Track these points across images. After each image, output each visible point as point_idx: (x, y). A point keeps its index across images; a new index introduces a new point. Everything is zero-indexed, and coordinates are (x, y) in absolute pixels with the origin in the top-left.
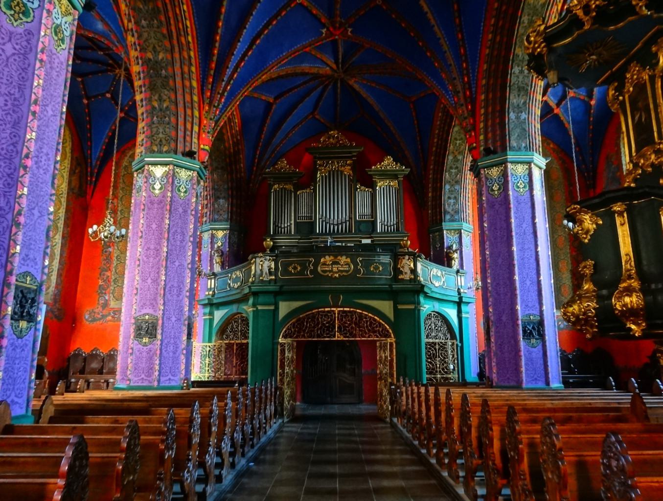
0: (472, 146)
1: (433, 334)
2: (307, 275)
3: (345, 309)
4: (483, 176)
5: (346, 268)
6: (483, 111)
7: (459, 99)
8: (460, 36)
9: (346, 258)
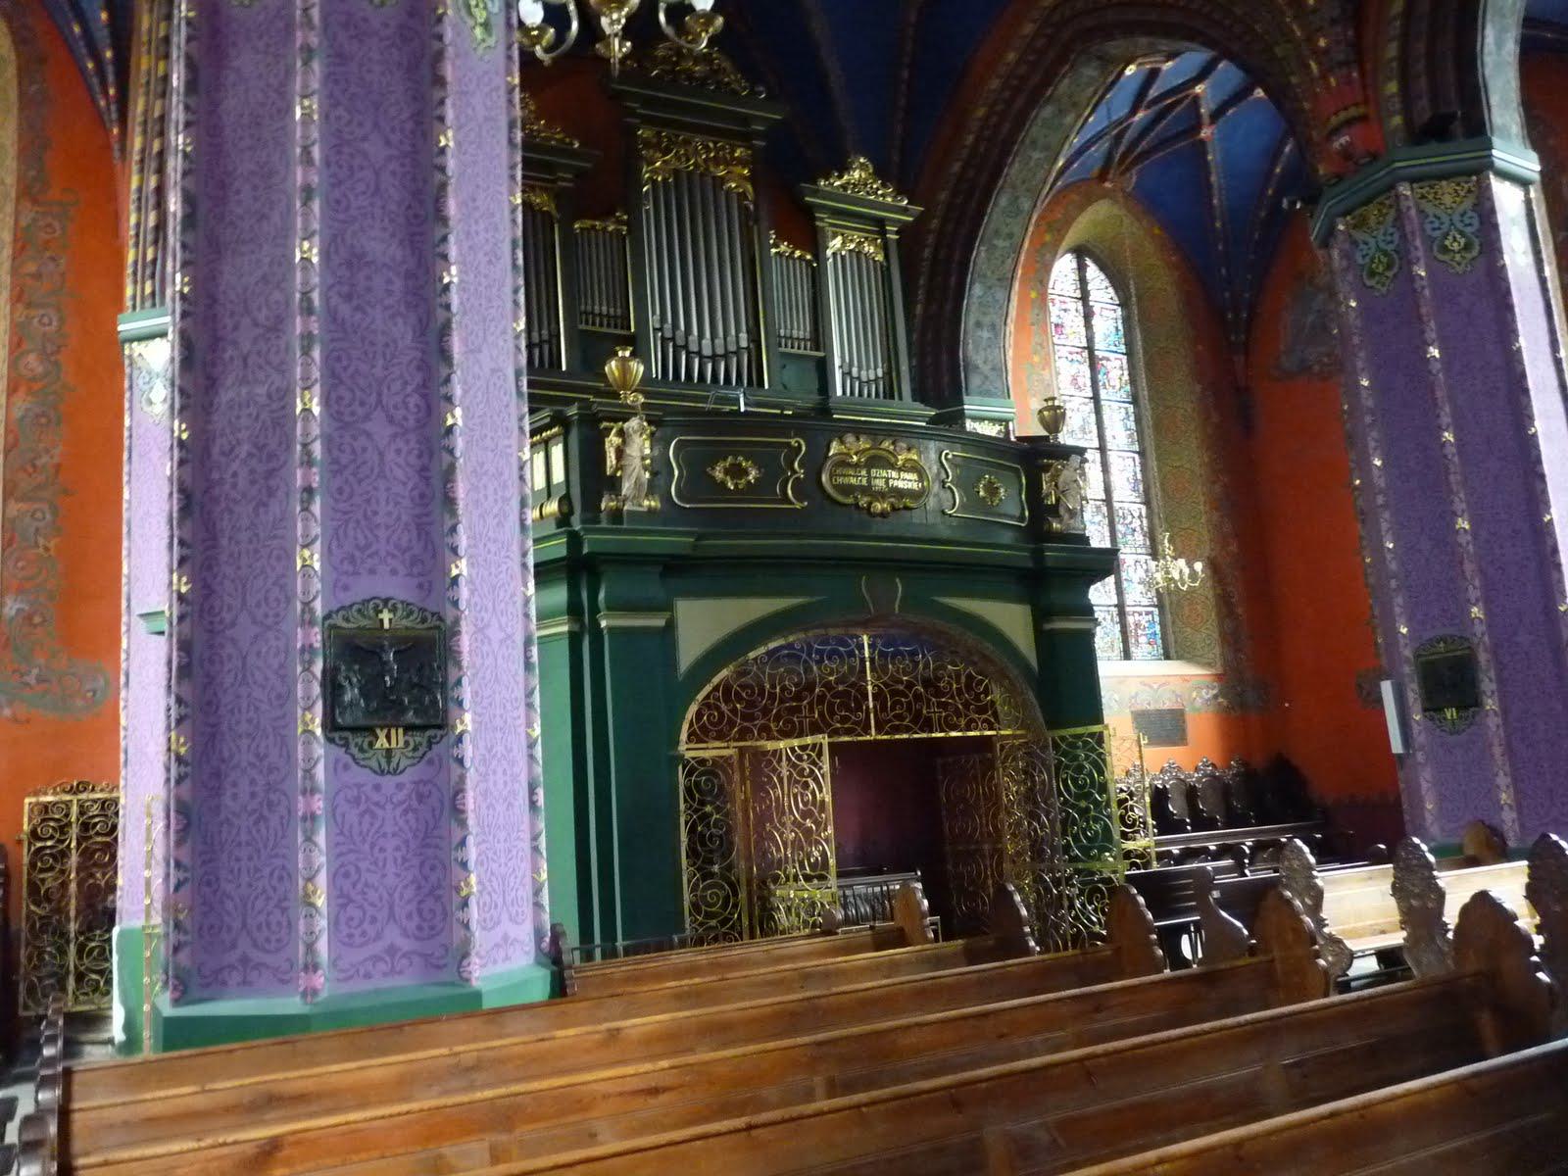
2: (786, 500)
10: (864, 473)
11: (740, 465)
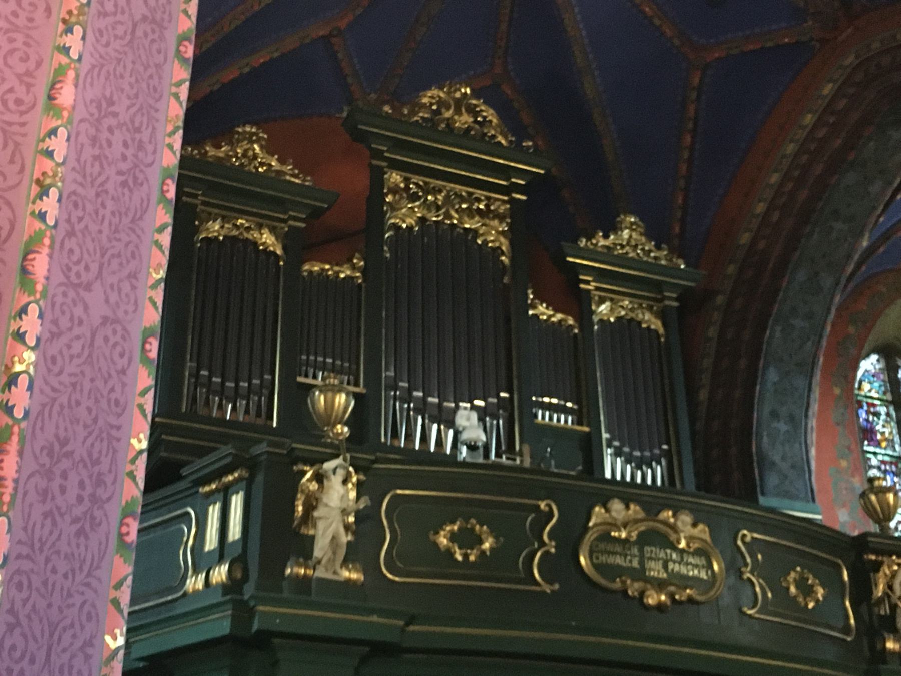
10: (635, 551)
11: (473, 529)
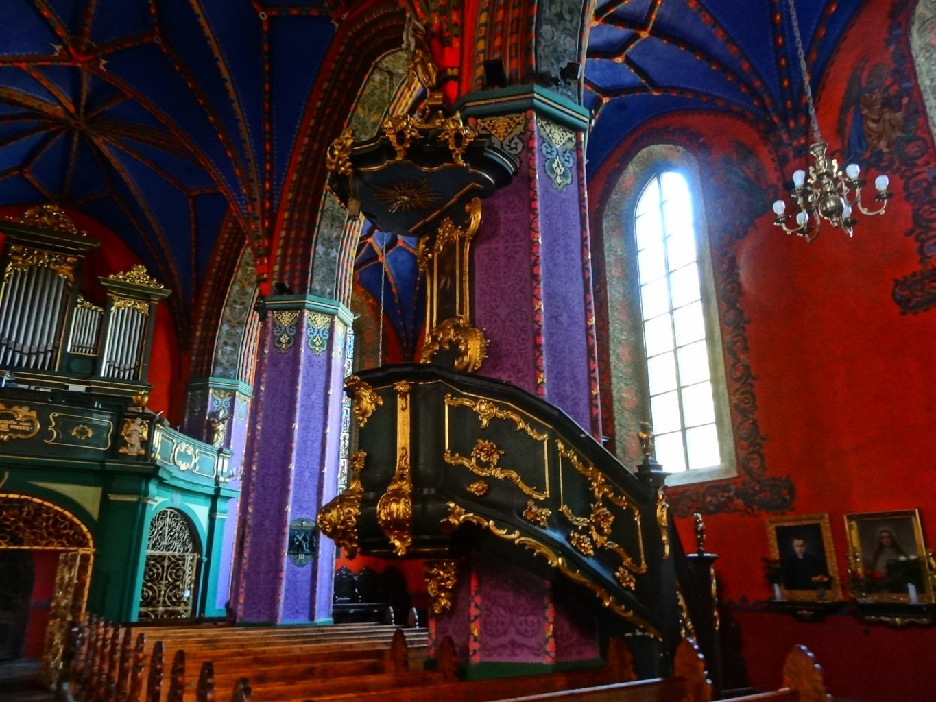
0: (261, 277)
1: (165, 543)
3: (11, 496)
4: (270, 320)
5: (25, 427)
6: (283, 233)
7: (253, 209)
8: (267, 127)
9: (29, 411)
